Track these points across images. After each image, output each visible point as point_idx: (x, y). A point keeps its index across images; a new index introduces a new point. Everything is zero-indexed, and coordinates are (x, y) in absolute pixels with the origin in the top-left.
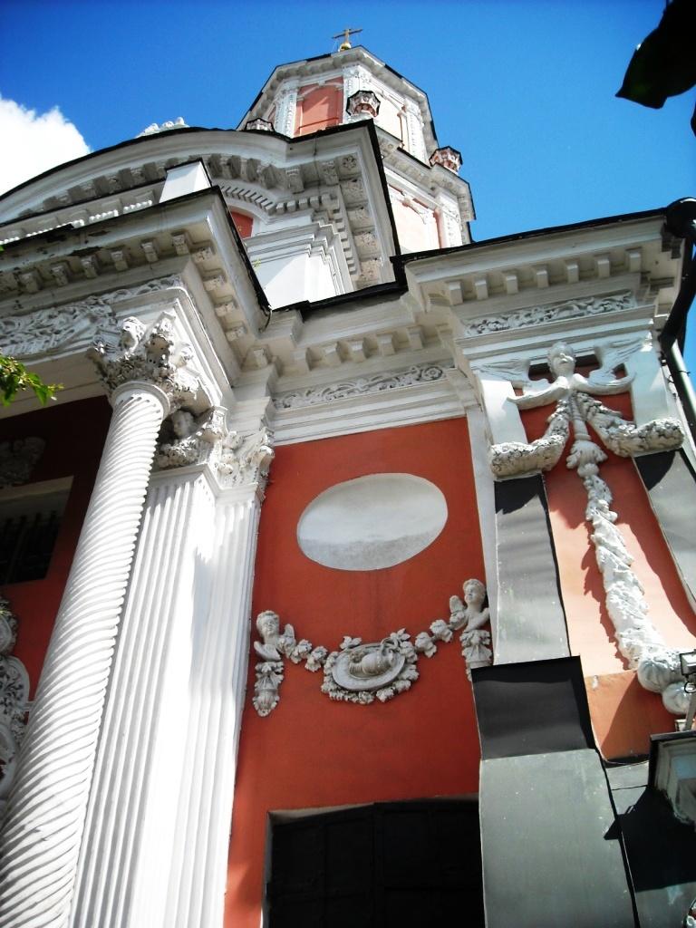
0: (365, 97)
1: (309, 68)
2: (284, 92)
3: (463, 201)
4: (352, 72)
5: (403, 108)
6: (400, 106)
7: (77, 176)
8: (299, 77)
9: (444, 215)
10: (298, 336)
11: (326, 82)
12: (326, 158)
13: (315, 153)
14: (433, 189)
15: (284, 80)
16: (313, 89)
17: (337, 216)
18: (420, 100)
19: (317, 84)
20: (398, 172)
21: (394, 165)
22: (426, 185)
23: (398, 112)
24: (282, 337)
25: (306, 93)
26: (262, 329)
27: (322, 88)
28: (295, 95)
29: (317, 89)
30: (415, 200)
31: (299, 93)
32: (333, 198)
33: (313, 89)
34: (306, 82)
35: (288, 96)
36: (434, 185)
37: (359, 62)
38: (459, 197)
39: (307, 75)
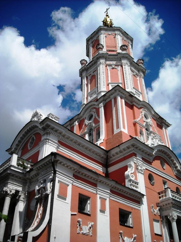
0: (99, 46)
1: (92, 36)
2: (89, 45)
3: (128, 58)
4: (100, 33)
5: (115, 35)
6: (114, 34)
7: (20, 135)
8: (91, 39)
9: (123, 65)
10: (29, 175)
11: (97, 38)
12: (44, 125)
13: (43, 124)
14: (120, 59)
15: (89, 41)
16: (94, 41)
17: (51, 132)
18: (119, 29)
19: (95, 40)
20: (111, 60)
21: (109, 59)
22: (119, 59)
23: (113, 37)
24: (27, 176)
25: (93, 43)
26: (25, 176)
27: (96, 40)
28: (91, 45)
29: (95, 41)
30: (115, 66)
31: (92, 44)
32: (48, 130)
33: (94, 41)
34: (93, 40)
35: (90, 46)
36: (120, 58)
37: (101, 30)
38: (127, 57)
39: (93, 38)
